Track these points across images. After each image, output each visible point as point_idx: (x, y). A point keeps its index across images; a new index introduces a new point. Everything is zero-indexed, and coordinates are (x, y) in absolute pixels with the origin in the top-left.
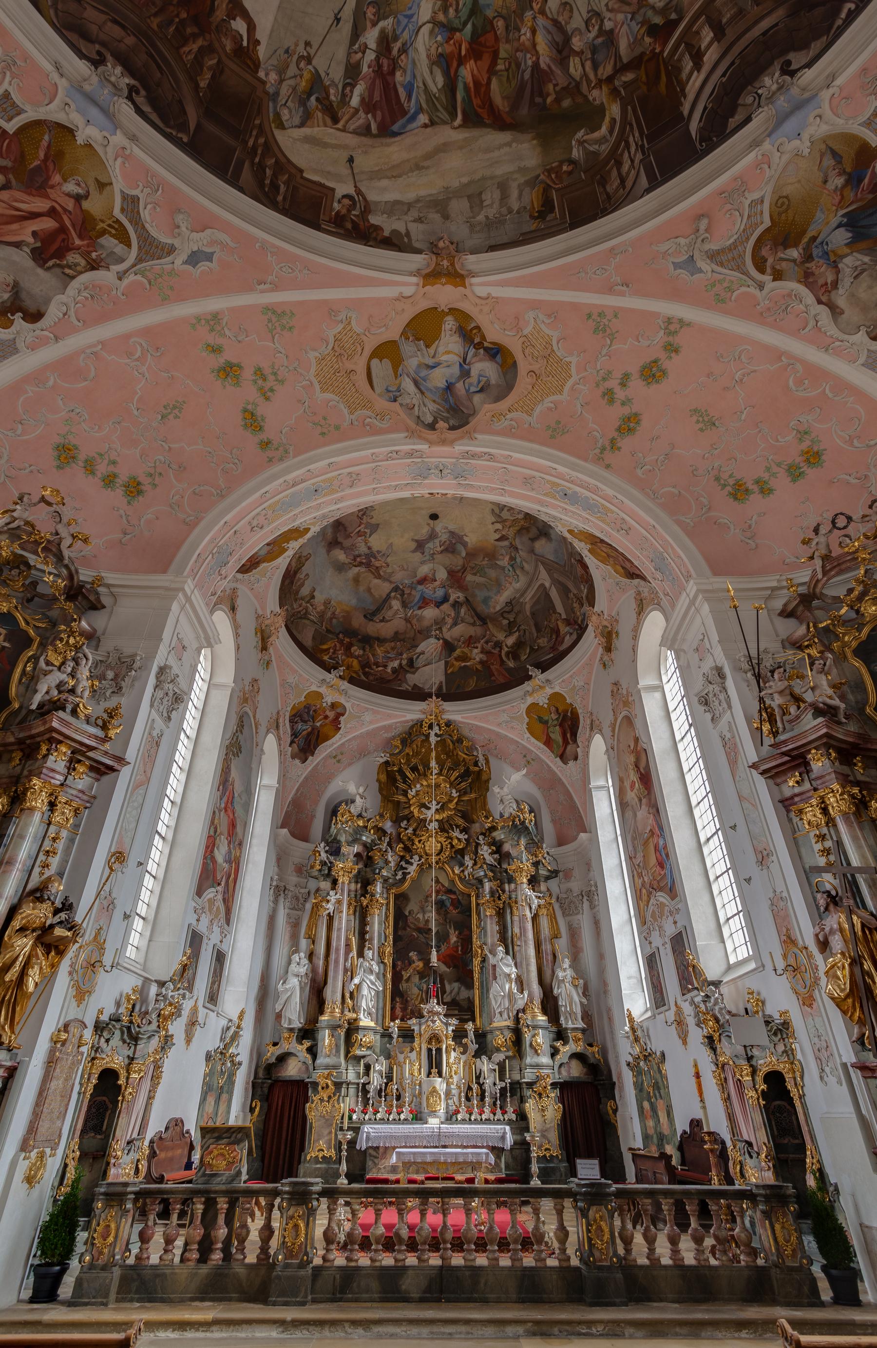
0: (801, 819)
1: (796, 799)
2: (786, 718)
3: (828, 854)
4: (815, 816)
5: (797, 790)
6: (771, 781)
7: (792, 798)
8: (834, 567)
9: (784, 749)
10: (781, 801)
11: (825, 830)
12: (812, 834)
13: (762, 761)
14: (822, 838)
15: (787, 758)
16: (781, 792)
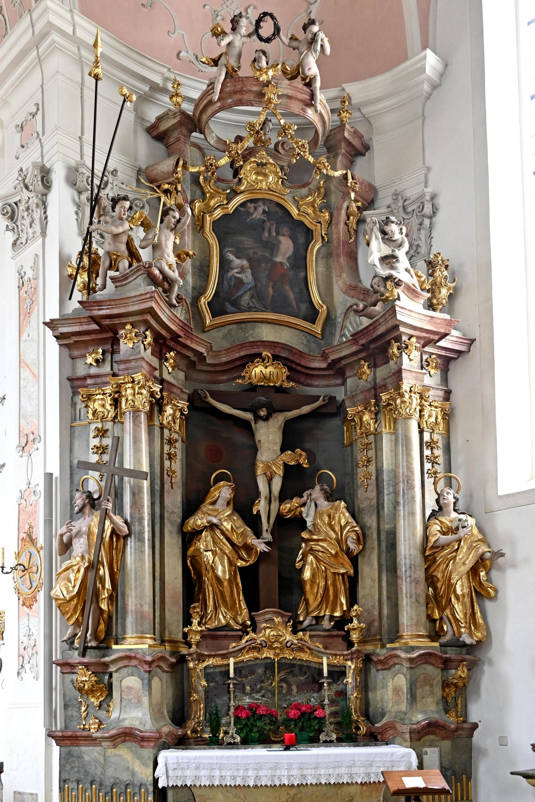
0: (87, 406)
1: (89, 381)
2: (111, 273)
3: (103, 453)
4: (103, 406)
5: (93, 371)
6: (66, 351)
7: (85, 378)
8: (236, 92)
9: (96, 313)
10: (70, 379)
11: (109, 425)
12: (93, 427)
13: (64, 319)
14: (102, 433)
15: (95, 327)
16: (74, 368)
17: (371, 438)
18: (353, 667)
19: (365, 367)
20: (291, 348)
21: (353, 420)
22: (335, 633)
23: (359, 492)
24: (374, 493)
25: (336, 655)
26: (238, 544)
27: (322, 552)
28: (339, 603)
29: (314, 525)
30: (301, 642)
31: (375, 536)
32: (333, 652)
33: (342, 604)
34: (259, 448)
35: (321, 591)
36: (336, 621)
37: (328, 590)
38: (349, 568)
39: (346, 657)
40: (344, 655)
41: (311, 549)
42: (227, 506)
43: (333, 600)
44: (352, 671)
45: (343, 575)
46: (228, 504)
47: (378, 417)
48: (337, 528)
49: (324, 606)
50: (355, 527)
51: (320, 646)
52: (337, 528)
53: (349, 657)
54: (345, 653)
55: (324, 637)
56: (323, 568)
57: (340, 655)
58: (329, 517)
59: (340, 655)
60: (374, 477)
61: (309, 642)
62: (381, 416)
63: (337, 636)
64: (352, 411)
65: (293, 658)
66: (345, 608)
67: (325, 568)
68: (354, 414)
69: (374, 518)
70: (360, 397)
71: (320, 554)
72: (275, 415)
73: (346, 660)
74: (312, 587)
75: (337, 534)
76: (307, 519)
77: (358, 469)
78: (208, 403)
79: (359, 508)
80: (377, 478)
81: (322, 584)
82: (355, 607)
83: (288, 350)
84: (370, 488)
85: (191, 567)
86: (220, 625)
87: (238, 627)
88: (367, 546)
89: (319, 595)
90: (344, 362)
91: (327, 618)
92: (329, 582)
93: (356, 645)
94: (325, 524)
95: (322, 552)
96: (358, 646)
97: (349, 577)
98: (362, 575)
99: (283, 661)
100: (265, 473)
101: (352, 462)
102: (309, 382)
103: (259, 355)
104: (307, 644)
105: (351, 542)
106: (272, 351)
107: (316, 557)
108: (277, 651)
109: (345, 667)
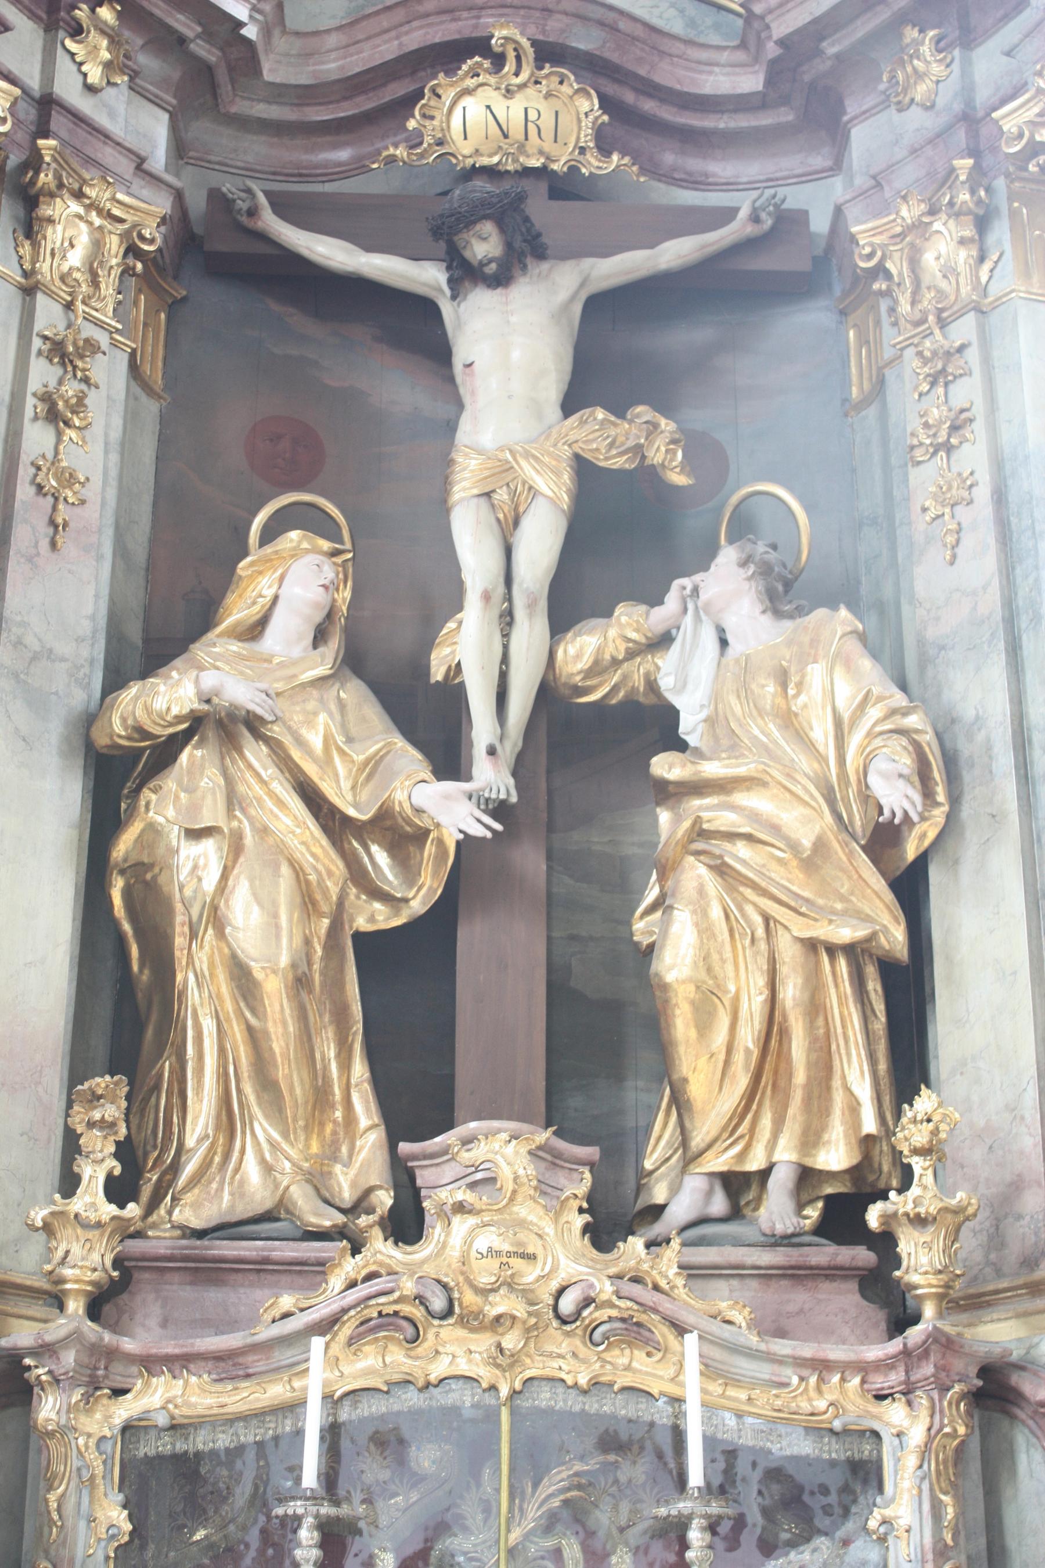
17: (964, 329)
18: (917, 1435)
19: (926, 49)
20: (612, 15)
21: (880, 271)
22: (825, 1253)
23: (919, 571)
24: (990, 562)
25: (822, 1367)
26: (352, 812)
27: (749, 838)
28: (839, 1098)
29: (711, 721)
30: (636, 1290)
31: (1005, 761)
32: (807, 1350)
33: (854, 1108)
34: (467, 400)
35: (748, 1037)
36: (829, 1199)
37: (784, 1033)
38: (886, 919)
39: (880, 1382)
40: (864, 1369)
41: (700, 833)
42: (315, 645)
43: (808, 1086)
44: (911, 1461)
45: (851, 950)
46: (320, 636)
47: (991, 239)
48: (822, 733)
49: (766, 1122)
50: (905, 712)
51: (739, 1317)
52: (822, 733)
53: (895, 1378)
54: (875, 1352)
55: (766, 1275)
56: (758, 920)
57: (846, 1368)
58: (783, 681)
59: (846, 1368)
60: (983, 493)
61: (681, 1292)
62: (1000, 233)
63: (832, 1273)
64: (876, 231)
65: (595, 1384)
66: (870, 1125)
67: (767, 919)
68: (883, 246)
69: (997, 671)
70: (910, 173)
71: (742, 849)
72: (537, 269)
73: (880, 1397)
74: (704, 1024)
75: (823, 759)
76: (677, 701)
77: (913, 473)
78: (263, 237)
79: (921, 643)
80: (1000, 498)
81: (754, 1004)
82: (925, 1102)
83: (601, 24)
84: (968, 542)
85: (127, 927)
86: (243, 1211)
87: (330, 1219)
88: (966, 811)
89: (739, 1058)
90: (831, 47)
91: (781, 1181)
92: (791, 992)
93: (929, 1311)
94: (761, 712)
95: (749, 838)
96: (940, 1315)
97: (888, 968)
98: (948, 959)
99: (544, 1397)
100: (488, 495)
101: (885, 441)
102: (694, 164)
103: (480, 46)
104: (666, 1305)
105: (885, 776)
106: (532, 30)
107: (721, 869)
108: (511, 1341)
109: (876, 1435)
